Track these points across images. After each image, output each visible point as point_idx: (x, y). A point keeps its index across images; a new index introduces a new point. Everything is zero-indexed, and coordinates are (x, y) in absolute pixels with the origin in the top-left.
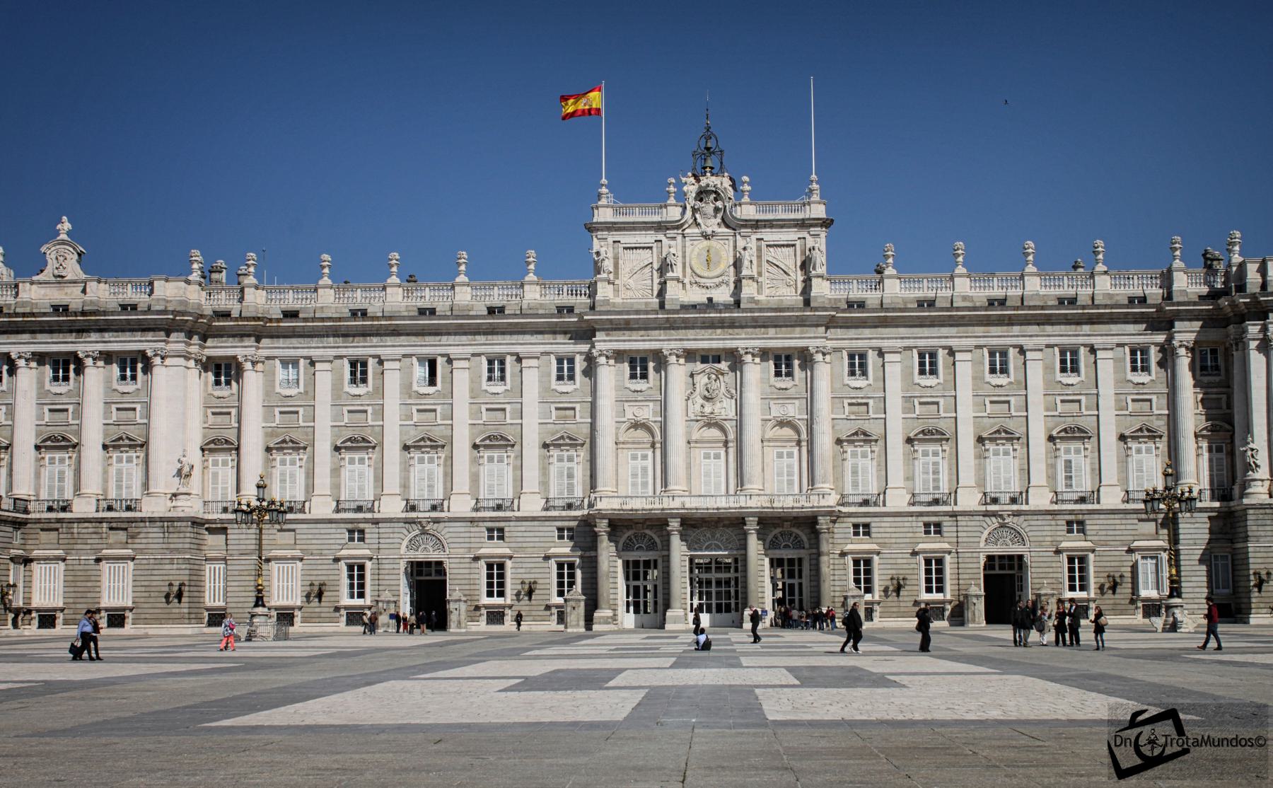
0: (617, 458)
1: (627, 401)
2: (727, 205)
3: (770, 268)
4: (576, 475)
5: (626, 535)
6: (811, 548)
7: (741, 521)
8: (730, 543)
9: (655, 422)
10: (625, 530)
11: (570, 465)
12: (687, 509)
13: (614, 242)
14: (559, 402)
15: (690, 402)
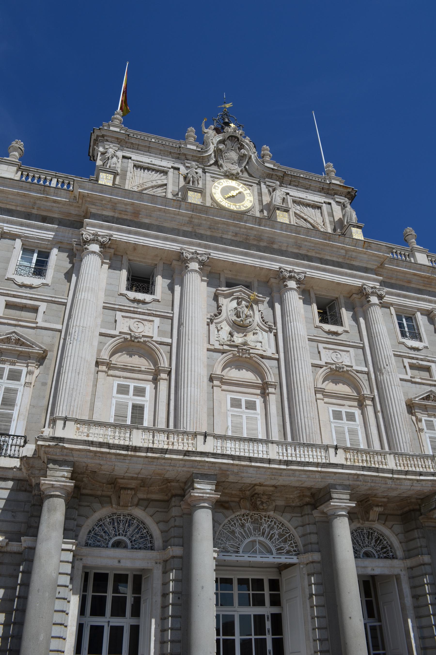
0: (95, 385)
1: (121, 310)
2: (253, 156)
3: (298, 220)
4: (18, 401)
5: (97, 515)
6: (406, 558)
7: (307, 499)
8: (285, 541)
9: (162, 343)
10: (96, 505)
11: (12, 384)
12: (232, 457)
13: (124, 157)
14: (14, 296)
15: (213, 327)
